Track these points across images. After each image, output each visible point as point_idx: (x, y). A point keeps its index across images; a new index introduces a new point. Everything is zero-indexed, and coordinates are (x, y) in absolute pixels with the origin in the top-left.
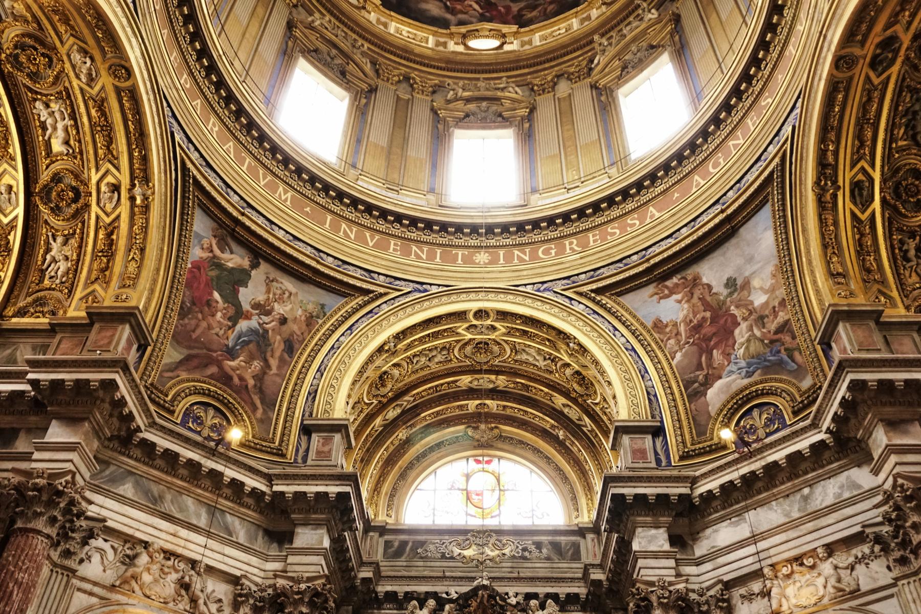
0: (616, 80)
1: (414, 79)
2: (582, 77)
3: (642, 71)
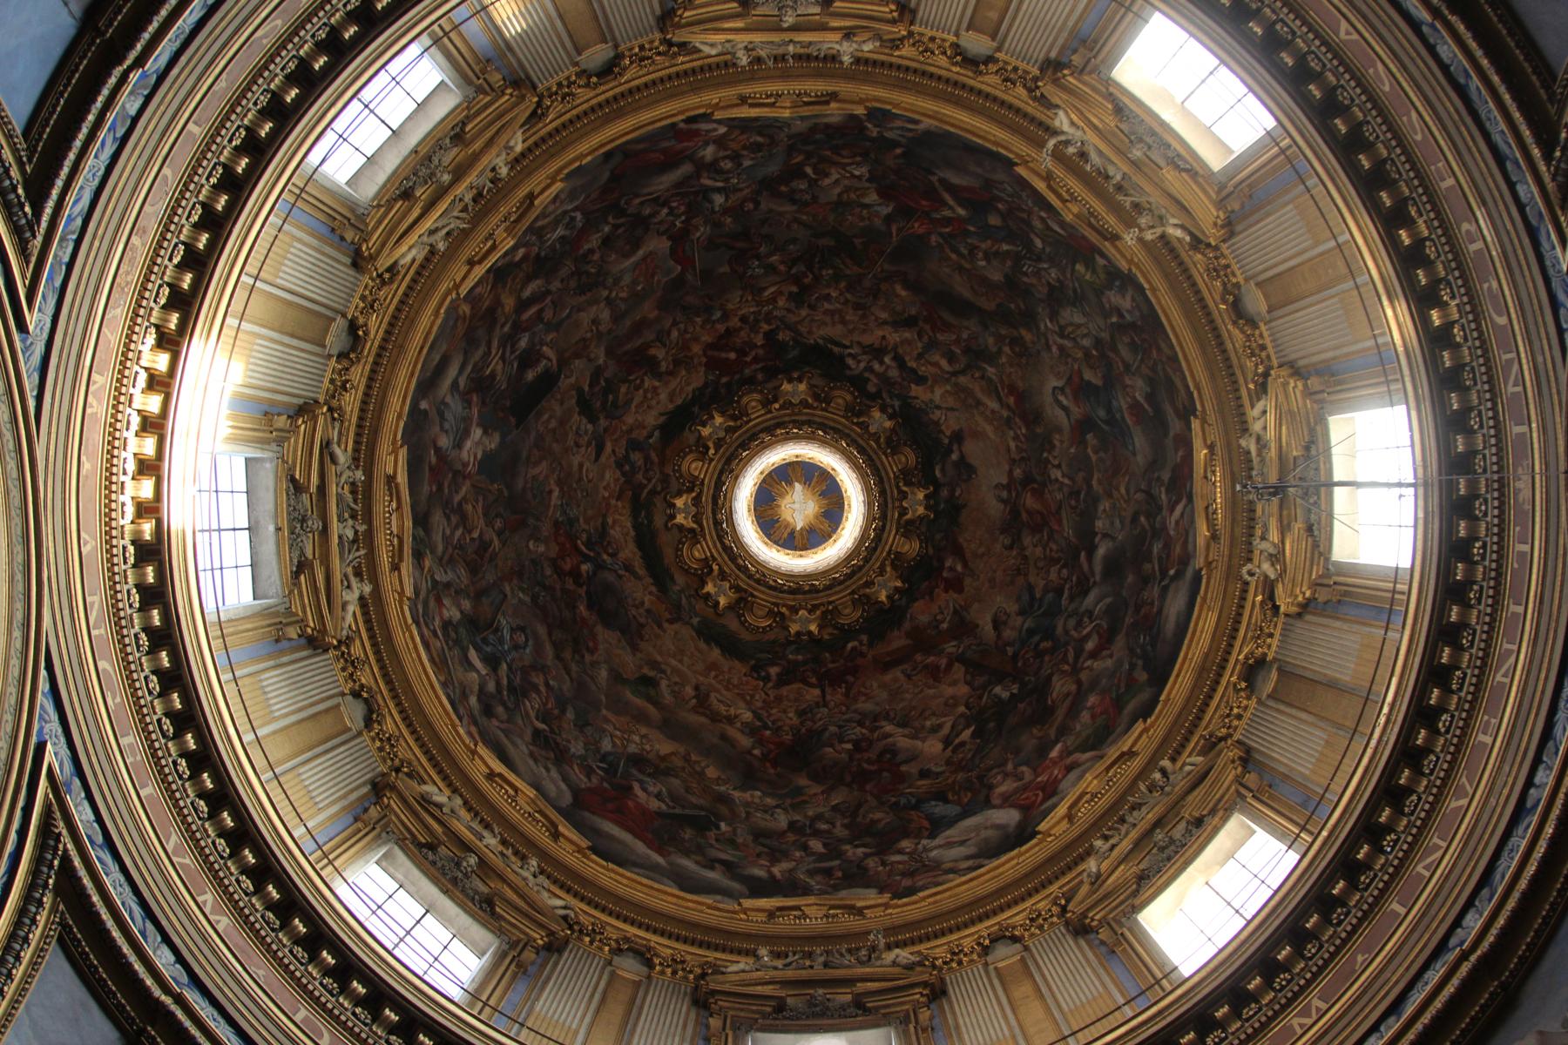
0: (1201, 180)
1: (1246, 658)
2: (1223, 262)
3: (1163, 124)
